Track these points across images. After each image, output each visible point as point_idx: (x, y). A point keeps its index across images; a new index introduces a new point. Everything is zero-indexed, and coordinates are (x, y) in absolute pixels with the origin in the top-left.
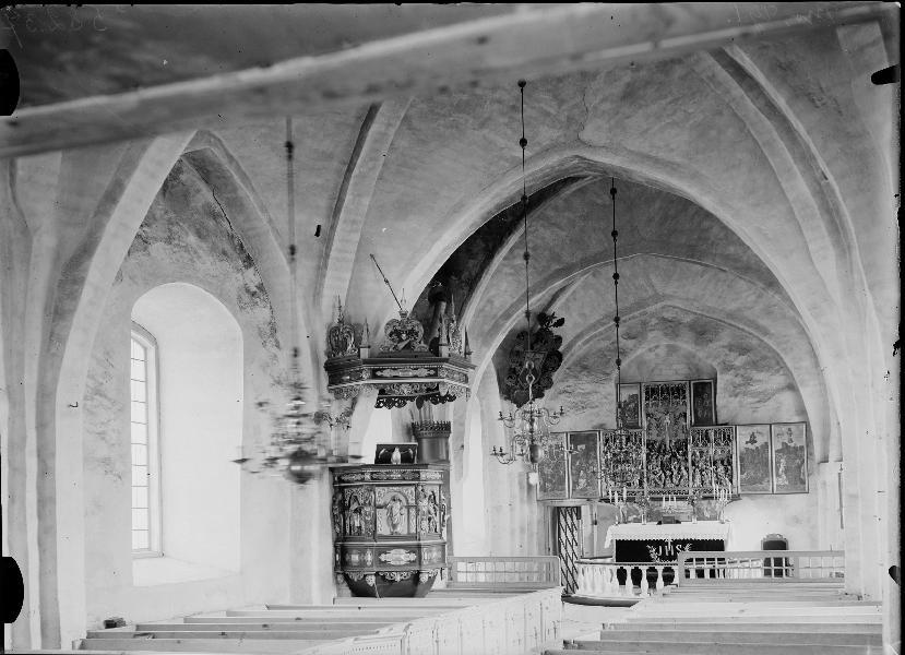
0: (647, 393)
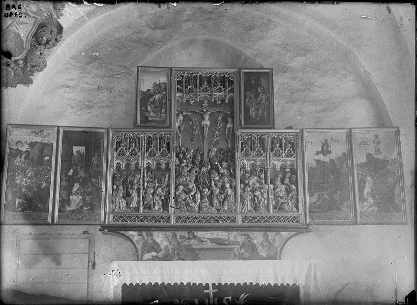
0: (180, 83)
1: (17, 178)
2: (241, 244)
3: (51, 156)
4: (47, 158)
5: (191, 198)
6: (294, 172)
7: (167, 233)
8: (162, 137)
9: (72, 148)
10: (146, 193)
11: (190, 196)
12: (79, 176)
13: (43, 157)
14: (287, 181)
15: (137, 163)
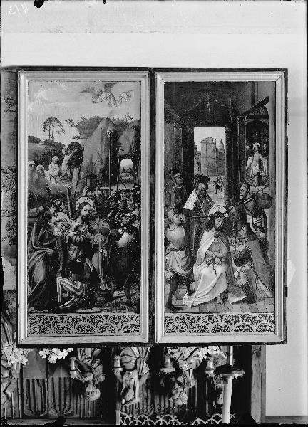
1: (54, 219)
3: (136, 156)
4: (126, 163)
12: (212, 211)
13: (116, 164)
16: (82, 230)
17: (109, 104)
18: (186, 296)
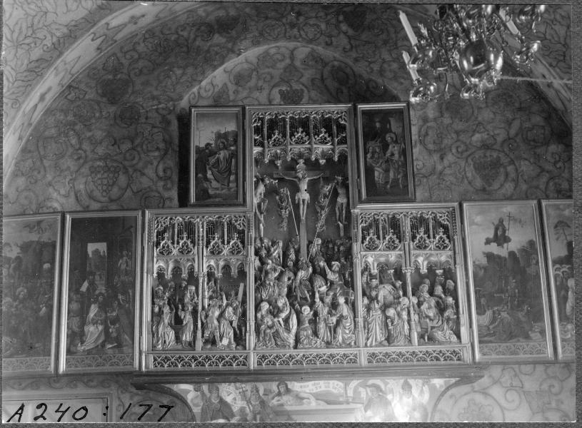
2: (366, 403)
3: (53, 262)
4: (46, 266)
5: (282, 322)
6: (449, 274)
7: (243, 385)
8: (230, 221)
9: (87, 245)
10: (207, 316)
11: (280, 320)
12: (97, 292)
13: (41, 266)
14: (439, 290)
15: (192, 268)
16: (19, 307)
17: (39, 233)
18: (79, 345)
